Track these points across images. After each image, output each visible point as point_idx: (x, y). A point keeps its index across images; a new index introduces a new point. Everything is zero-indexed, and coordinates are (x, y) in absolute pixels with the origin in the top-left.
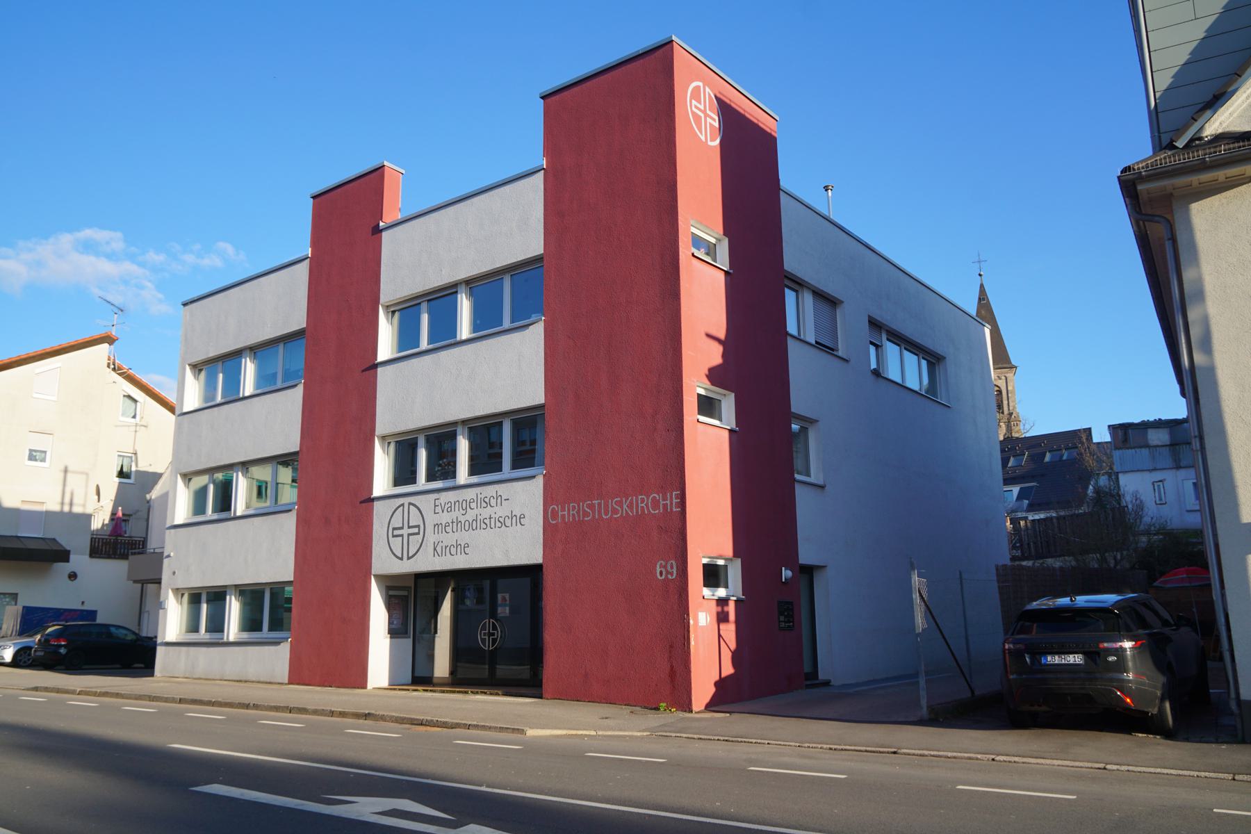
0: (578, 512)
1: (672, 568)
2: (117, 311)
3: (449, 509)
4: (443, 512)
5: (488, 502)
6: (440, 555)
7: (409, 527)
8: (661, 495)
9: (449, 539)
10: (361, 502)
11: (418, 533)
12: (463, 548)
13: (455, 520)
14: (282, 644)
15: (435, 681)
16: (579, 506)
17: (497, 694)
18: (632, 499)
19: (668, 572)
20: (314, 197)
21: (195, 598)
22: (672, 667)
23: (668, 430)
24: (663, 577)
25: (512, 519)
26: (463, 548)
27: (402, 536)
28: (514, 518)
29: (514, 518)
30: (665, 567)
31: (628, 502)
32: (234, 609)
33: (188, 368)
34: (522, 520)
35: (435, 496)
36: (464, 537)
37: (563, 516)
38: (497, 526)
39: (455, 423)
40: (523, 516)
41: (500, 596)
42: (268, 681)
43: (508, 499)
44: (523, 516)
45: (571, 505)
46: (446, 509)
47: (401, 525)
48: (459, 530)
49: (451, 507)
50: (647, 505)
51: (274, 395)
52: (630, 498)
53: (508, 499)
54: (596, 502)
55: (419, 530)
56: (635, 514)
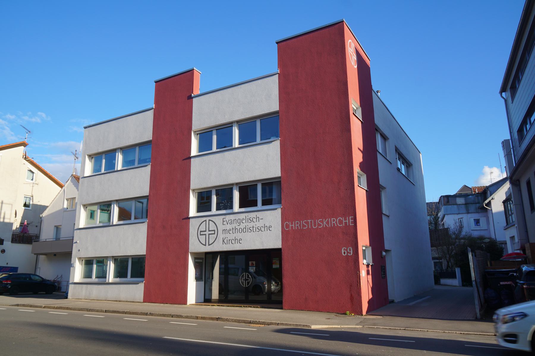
0: (300, 225)
1: (350, 250)
2: (27, 132)
4: (227, 224)
5: (252, 220)
6: (226, 244)
7: (209, 231)
8: (343, 218)
9: (231, 236)
10: (183, 219)
11: (214, 234)
12: (239, 241)
13: (234, 228)
14: (139, 284)
15: (212, 301)
16: (300, 222)
17: (257, 307)
18: (328, 220)
19: (348, 252)
20: (156, 82)
21: (89, 262)
22: (351, 295)
23: (346, 189)
24: (346, 254)
25: (265, 228)
26: (239, 241)
27: (205, 235)
28: (266, 227)
29: (266, 227)
30: (347, 250)
31: (326, 221)
32: (111, 268)
33: (87, 157)
34: (270, 228)
36: (239, 236)
37: (292, 227)
38: (257, 231)
39: (233, 184)
40: (270, 227)
41: (250, 263)
42: (132, 301)
43: (262, 219)
44: (270, 227)
45: (296, 222)
46: (229, 223)
47: (205, 230)
48: (236, 232)
49: (232, 222)
50: (336, 222)
51: (134, 169)
52: (327, 219)
53: (262, 219)
54: (309, 221)
55: (215, 232)
56: (330, 226)
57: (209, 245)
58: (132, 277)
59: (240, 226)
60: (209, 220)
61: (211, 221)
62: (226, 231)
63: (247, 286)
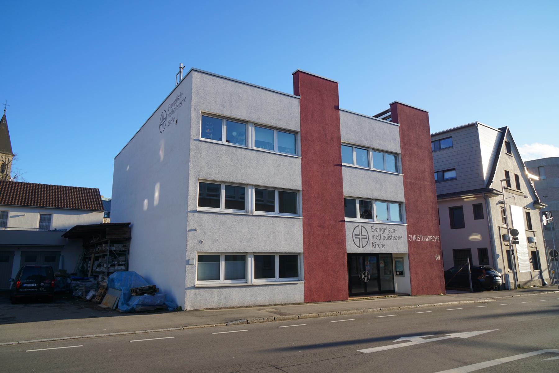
3: (377, 231)
4: (375, 231)
9: (378, 241)
10: (339, 221)
12: (382, 245)
13: (380, 235)
19: (438, 258)
22: (441, 283)
26: (382, 245)
34: (401, 238)
35: (372, 225)
36: (383, 242)
40: (401, 237)
41: (366, 262)
44: (401, 237)
48: (381, 239)
49: (378, 230)
55: (366, 237)
57: (363, 247)
58: (281, 276)
59: (384, 235)
60: (361, 226)
61: (363, 227)
62: (374, 237)
63: (367, 281)
